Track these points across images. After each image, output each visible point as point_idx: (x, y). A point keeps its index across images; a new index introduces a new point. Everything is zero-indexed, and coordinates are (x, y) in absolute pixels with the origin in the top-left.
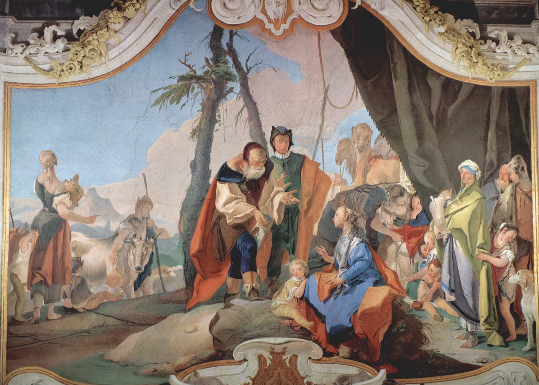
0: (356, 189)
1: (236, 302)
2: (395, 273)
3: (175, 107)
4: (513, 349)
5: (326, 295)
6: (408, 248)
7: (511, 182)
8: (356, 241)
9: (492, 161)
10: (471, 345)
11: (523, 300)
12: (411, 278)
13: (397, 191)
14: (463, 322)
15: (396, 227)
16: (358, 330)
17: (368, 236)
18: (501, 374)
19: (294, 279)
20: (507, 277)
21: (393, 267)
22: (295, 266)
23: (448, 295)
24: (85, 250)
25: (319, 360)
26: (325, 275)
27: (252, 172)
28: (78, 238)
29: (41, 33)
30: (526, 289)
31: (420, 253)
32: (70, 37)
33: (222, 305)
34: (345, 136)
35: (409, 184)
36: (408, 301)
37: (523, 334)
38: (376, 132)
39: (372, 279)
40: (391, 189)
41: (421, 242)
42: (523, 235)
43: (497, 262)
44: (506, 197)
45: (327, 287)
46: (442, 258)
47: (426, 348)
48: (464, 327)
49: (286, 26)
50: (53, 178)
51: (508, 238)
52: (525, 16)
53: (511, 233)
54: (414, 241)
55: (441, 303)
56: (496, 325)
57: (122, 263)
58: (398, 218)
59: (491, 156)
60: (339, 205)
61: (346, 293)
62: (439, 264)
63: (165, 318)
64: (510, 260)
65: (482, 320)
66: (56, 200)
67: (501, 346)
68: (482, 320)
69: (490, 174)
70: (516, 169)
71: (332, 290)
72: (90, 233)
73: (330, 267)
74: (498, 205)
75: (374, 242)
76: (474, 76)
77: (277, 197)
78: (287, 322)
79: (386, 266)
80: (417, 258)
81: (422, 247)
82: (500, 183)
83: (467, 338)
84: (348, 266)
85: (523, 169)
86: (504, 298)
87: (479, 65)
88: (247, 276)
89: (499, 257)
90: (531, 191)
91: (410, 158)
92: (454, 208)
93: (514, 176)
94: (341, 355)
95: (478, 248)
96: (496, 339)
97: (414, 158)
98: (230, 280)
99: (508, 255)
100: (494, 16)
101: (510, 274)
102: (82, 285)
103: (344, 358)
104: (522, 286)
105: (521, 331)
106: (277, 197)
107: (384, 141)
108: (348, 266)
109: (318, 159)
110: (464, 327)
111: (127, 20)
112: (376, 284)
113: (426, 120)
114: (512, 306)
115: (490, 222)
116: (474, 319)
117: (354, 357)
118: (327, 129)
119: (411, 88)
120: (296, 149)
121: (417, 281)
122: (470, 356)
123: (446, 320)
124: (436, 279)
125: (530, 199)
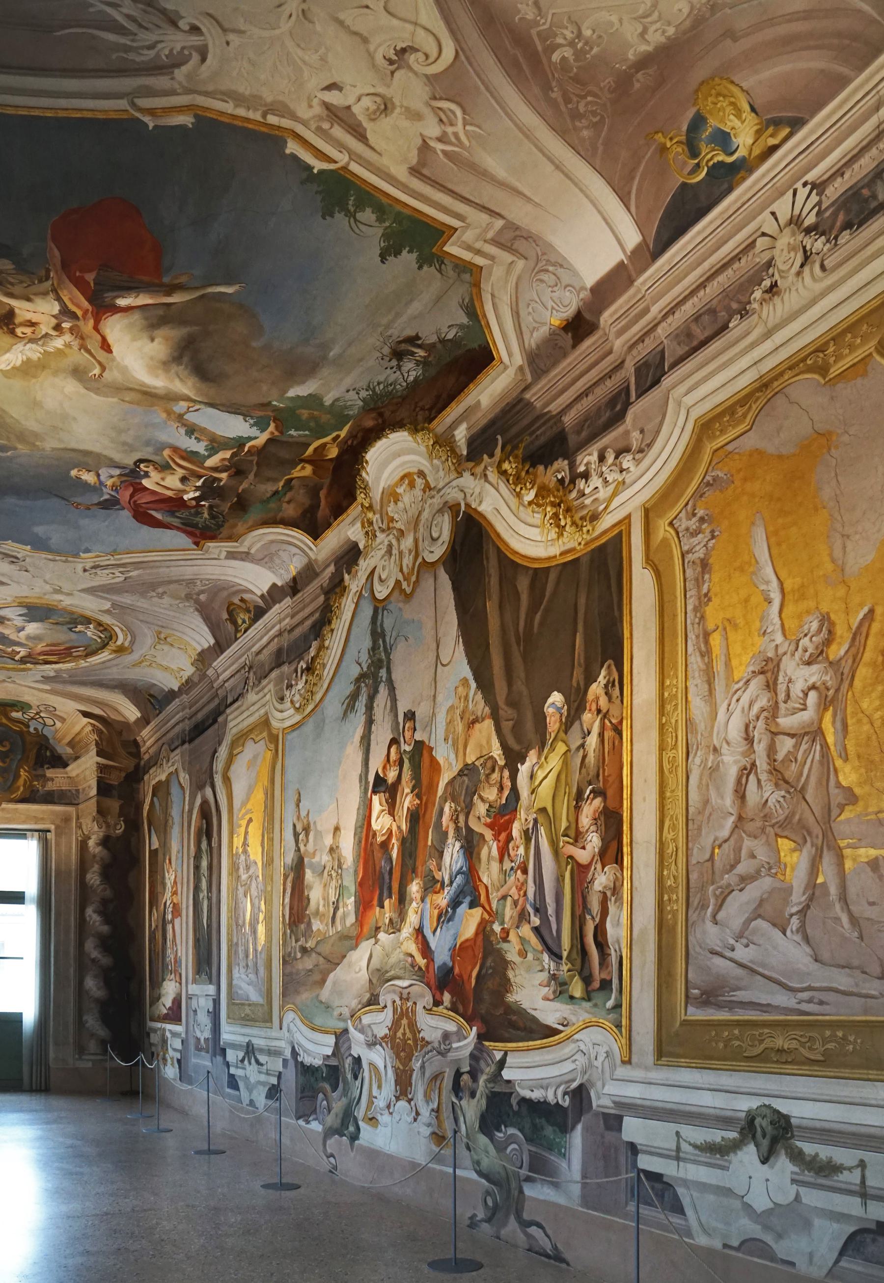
0: (458, 774)
1: (382, 936)
2: (487, 888)
3: (353, 715)
4: (595, 1005)
5: (435, 924)
6: (498, 848)
7: (599, 711)
8: (458, 845)
9: (578, 684)
10: (552, 997)
11: (608, 919)
12: (500, 894)
13: (489, 764)
14: (546, 957)
15: (489, 820)
16: (457, 970)
17: (466, 838)
18: (583, 1047)
19: (414, 905)
20: (592, 880)
21: (485, 880)
22: (414, 888)
23: (533, 918)
24: (311, 888)
25: (430, 1010)
26: (435, 897)
27: (391, 776)
28: (309, 875)
29: (296, 671)
30: (613, 899)
31: (509, 855)
32: (309, 669)
33: (373, 941)
34: (450, 703)
35: (500, 752)
36: (497, 928)
37: (608, 978)
38: (473, 685)
39: (468, 899)
40: (484, 765)
41: (510, 838)
42: (611, 805)
43: (583, 856)
44: (593, 741)
45: (436, 912)
46: (528, 860)
47: (511, 998)
48: (546, 967)
49: (414, 578)
50: (299, 817)
51: (595, 812)
52: (618, 407)
53: (598, 802)
54: (503, 836)
55: (526, 931)
56: (578, 966)
57: (326, 899)
58: (490, 806)
59: (578, 674)
60: (446, 801)
61: (449, 921)
62: (525, 872)
63: (344, 956)
64: (597, 850)
65: (565, 954)
66: (301, 837)
67: (583, 999)
68: (565, 954)
69: (577, 705)
70: (606, 686)
71: (440, 916)
72: (313, 867)
73: (439, 885)
74: (584, 757)
75: (471, 845)
76: (563, 549)
77: (407, 801)
78: (410, 959)
79: (480, 880)
80: (507, 865)
81: (511, 845)
82: (587, 717)
83: (548, 985)
84: (451, 883)
85: (613, 685)
86: (588, 917)
87: (567, 528)
88: (387, 903)
89: (584, 848)
90: (621, 722)
91: (501, 712)
92: (540, 775)
93: (603, 702)
94: (445, 1004)
95: (564, 836)
96: (577, 988)
97: (506, 712)
98: (378, 909)
99: (594, 841)
100: (584, 434)
101: (596, 875)
102: (309, 924)
103: (447, 1008)
104: (609, 894)
105: (604, 976)
106: (407, 801)
107: (479, 696)
108: (451, 883)
109: (432, 745)
110: (546, 967)
111: (332, 630)
112: (472, 905)
113: (515, 647)
114: (596, 928)
115: (574, 790)
116: (556, 956)
117: (453, 1009)
118: (440, 698)
119: (501, 607)
120: (418, 736)
121: (504, 898)
122: (550, 1013)
123: (530, 956)
124: (522, 893)
125: (620, 734)
